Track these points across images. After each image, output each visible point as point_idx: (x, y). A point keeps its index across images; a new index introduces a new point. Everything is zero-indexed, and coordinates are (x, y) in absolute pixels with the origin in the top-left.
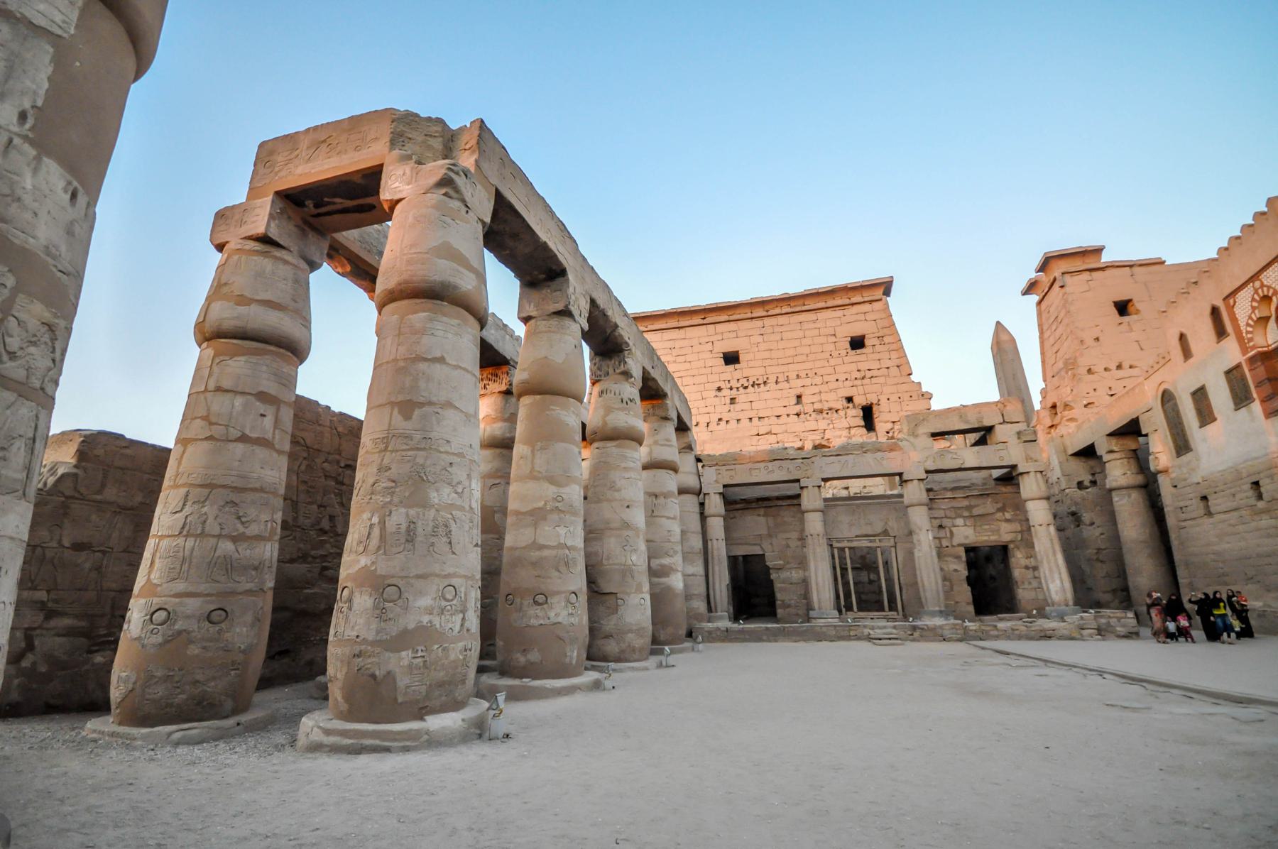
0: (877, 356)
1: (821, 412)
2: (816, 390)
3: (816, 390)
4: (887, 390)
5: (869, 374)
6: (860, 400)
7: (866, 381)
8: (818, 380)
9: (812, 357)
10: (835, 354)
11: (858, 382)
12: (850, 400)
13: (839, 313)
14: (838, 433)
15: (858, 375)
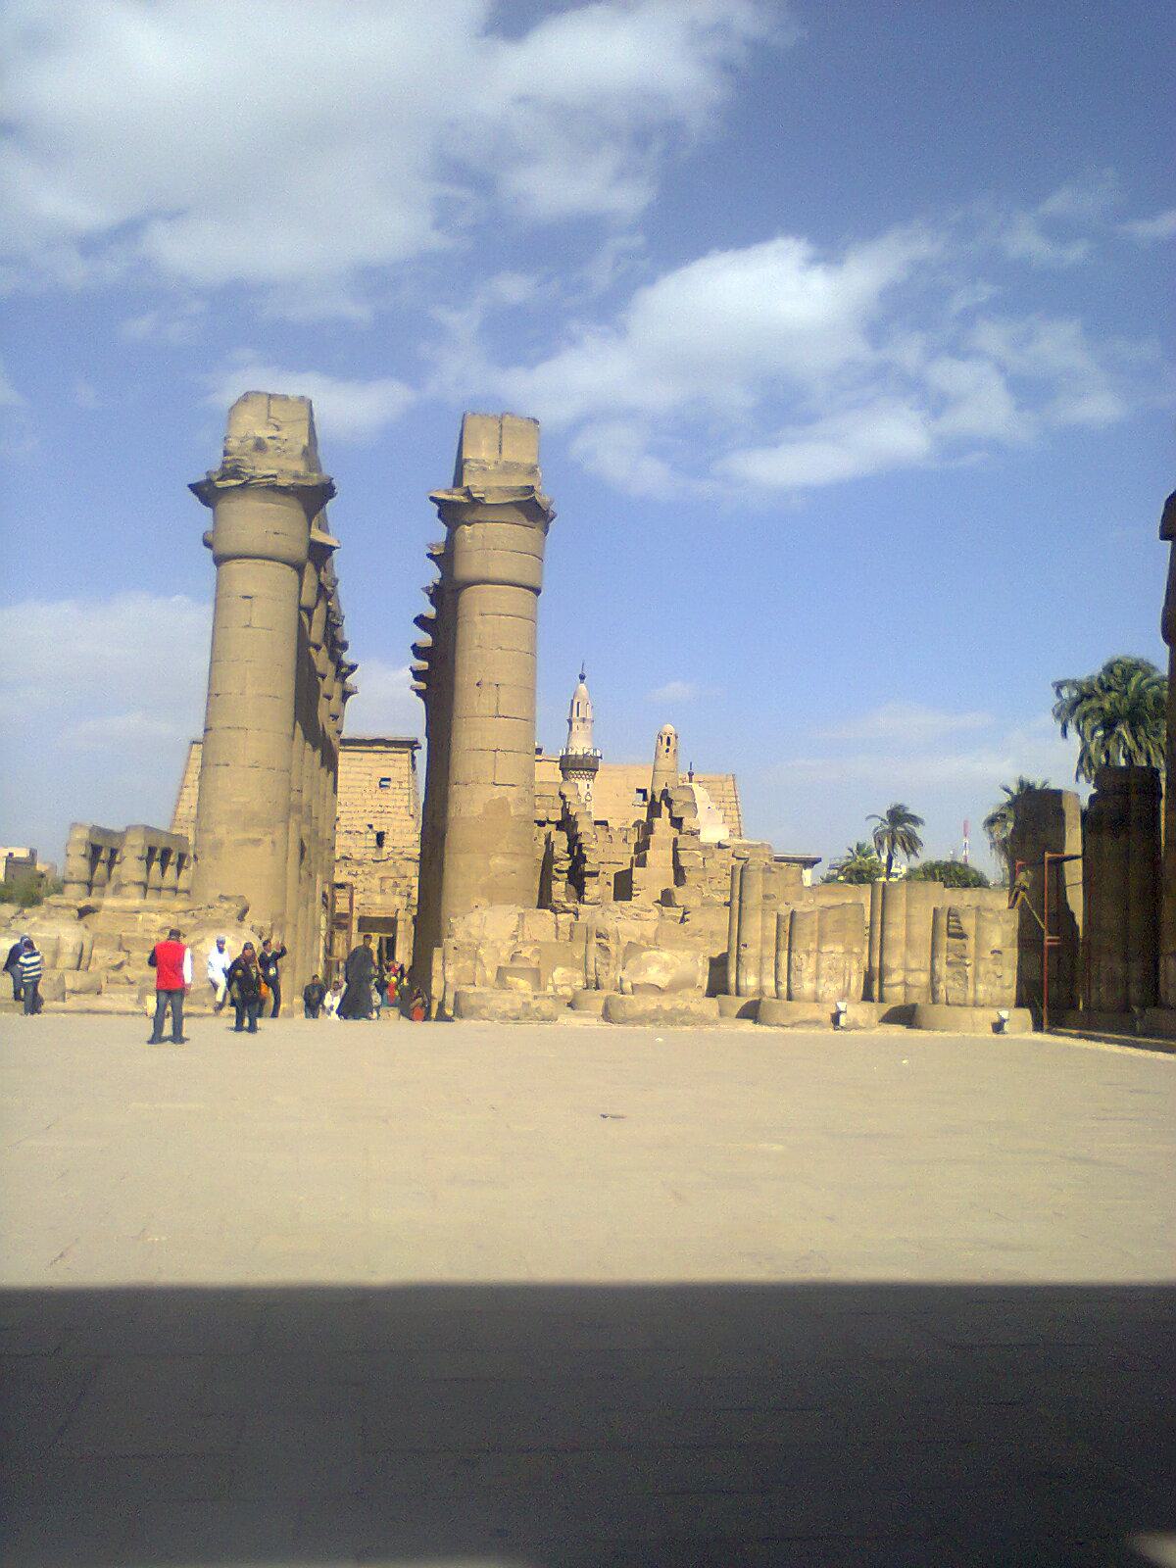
0: (395, 797)
1: (350, 833)
2: (349, 815)
3: (349, 815)
4: (396, 823)
5: (389, 810)
6: (376, 828)
7: (383, 815)
8: (352, 809)
9: (351, 790)
10: (368, 790)
11: (378, 815)
12: (371, 826)
13: (377, 756)
14: (358, 850)
15: (380, 809)
